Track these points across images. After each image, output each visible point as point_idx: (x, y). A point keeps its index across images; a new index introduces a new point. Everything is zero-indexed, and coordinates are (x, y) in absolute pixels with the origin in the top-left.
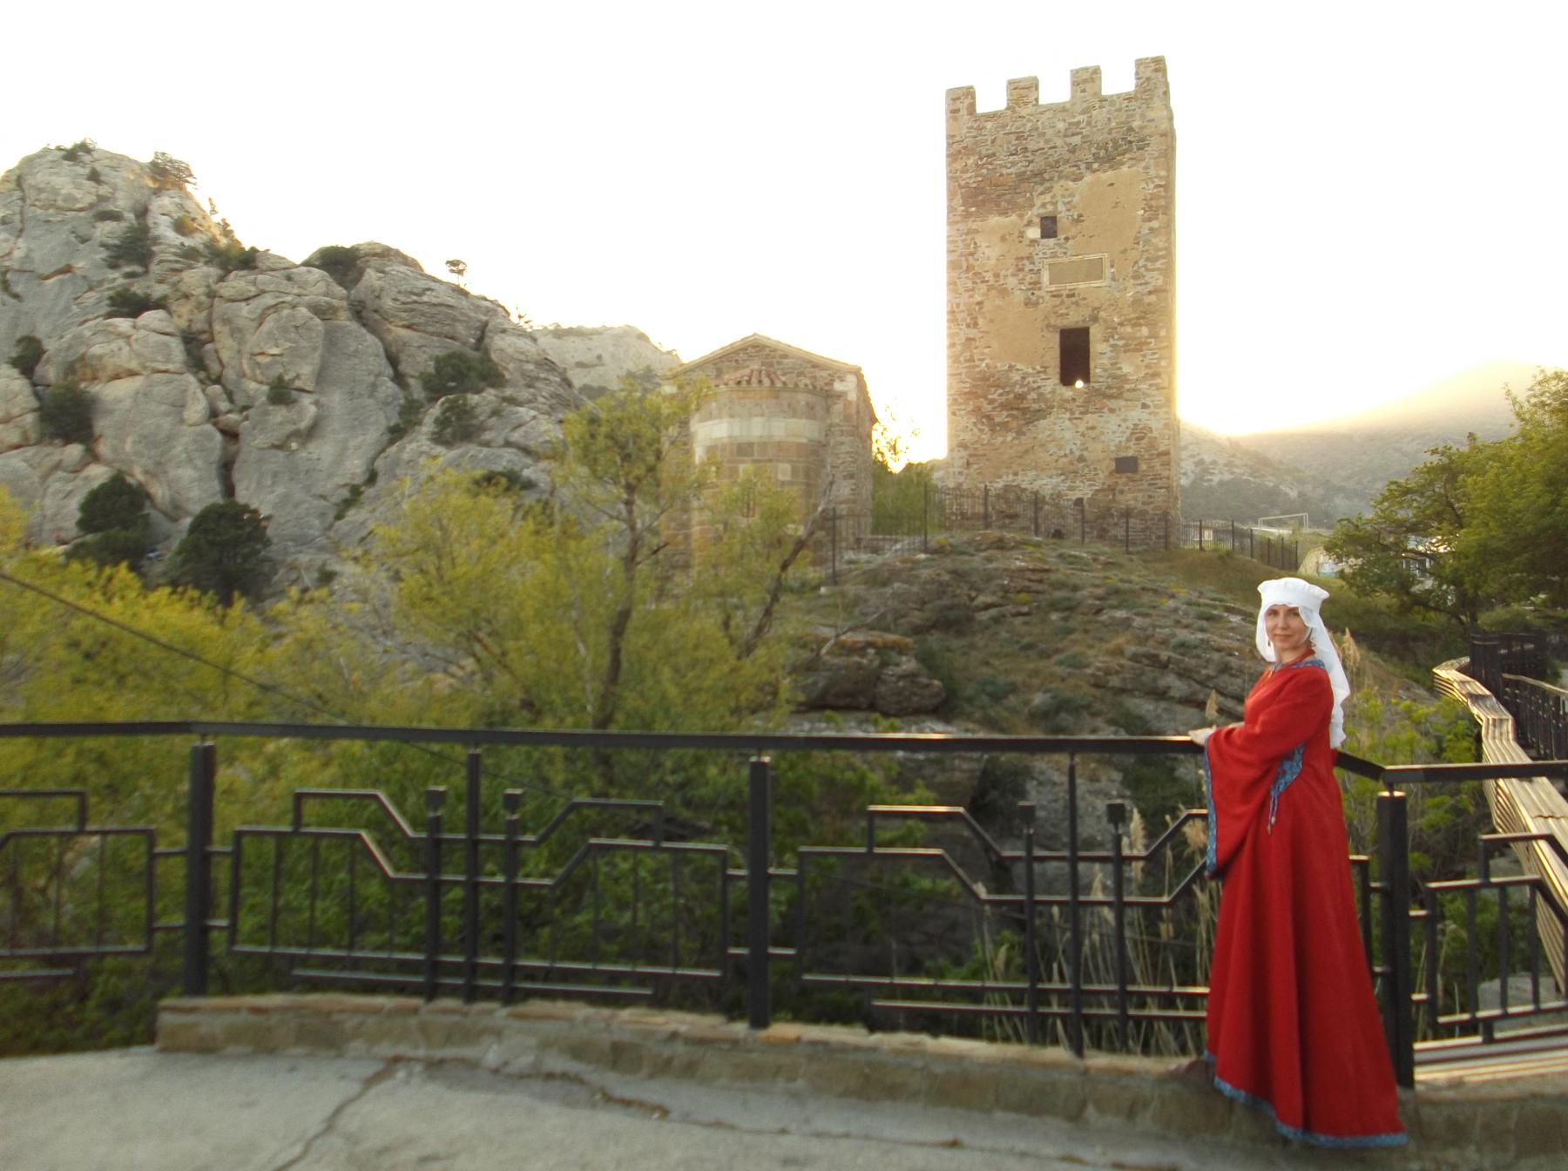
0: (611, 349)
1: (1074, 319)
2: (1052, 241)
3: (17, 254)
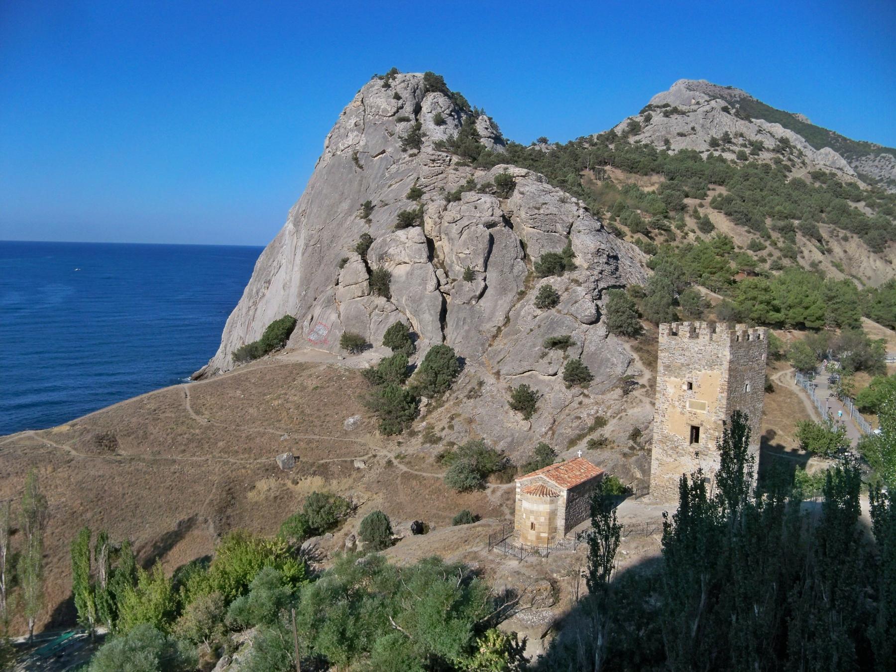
0: (701, 121)
1: (696, 423)
2: (690, 392)
3: (362, 143)
